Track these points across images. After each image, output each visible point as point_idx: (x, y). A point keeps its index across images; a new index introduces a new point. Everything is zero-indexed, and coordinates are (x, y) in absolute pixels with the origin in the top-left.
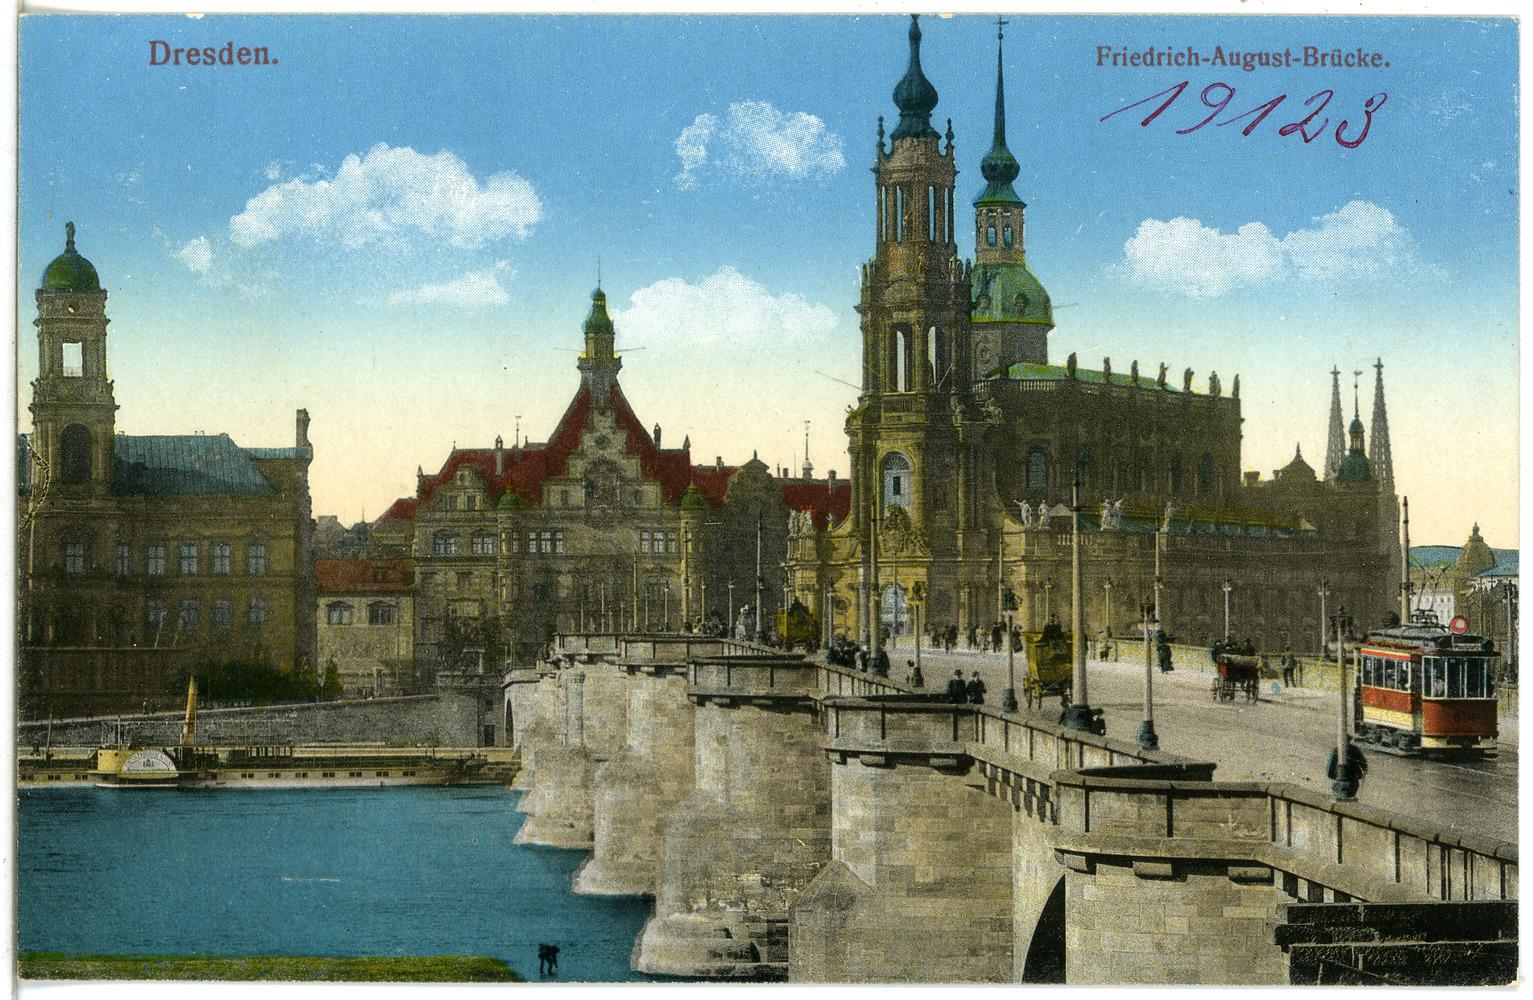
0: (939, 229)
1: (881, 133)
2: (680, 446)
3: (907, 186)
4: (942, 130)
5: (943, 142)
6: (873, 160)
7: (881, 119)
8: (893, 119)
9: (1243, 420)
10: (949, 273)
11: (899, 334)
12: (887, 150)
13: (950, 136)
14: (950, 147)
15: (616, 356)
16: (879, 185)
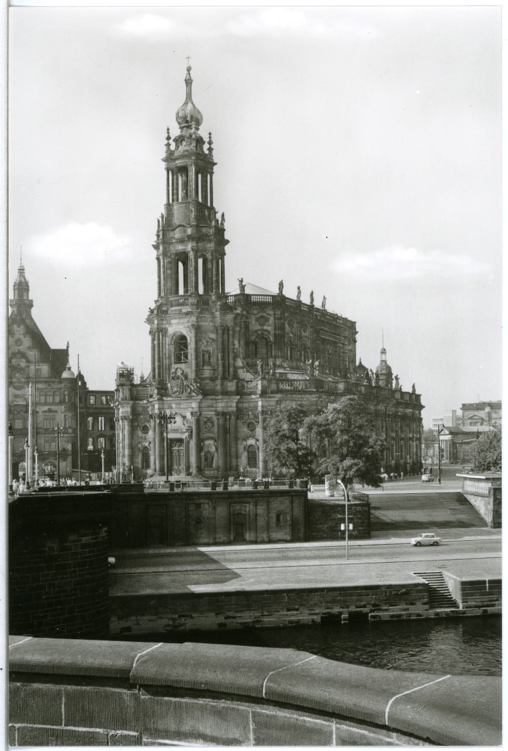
0: (205, 197)
1: (168, 138)
2: (65, 348)
3: (184, 170)
4: (206, 139)
5: (206, 147)
6: (164, 155)
7: (168, 130)
8: (176, 132)
9: (357, 332)
10: (211, 222)
11: (181, 265)
12: (173, 147)
13: (210, 143)
14: (210, 149)
15: (30, 299)
16: (168, 170)
